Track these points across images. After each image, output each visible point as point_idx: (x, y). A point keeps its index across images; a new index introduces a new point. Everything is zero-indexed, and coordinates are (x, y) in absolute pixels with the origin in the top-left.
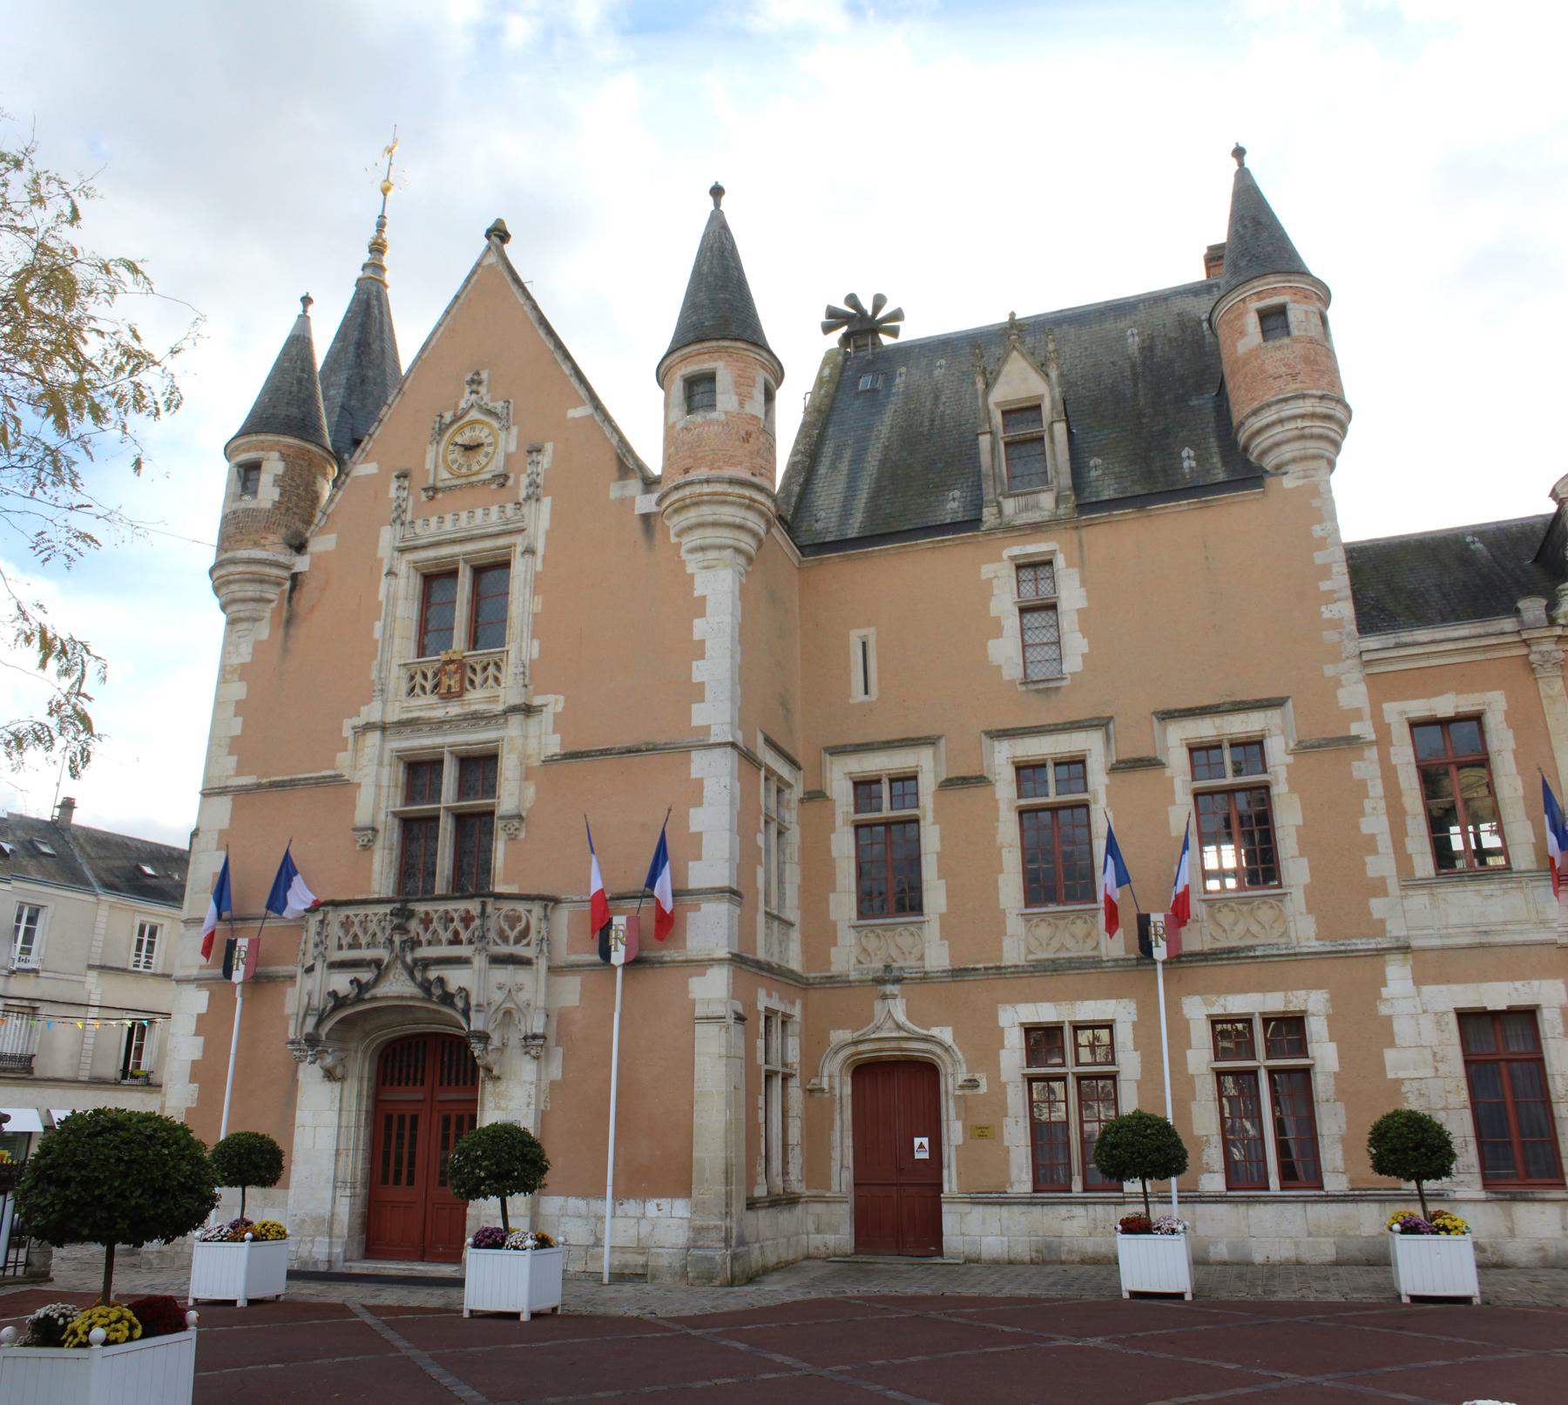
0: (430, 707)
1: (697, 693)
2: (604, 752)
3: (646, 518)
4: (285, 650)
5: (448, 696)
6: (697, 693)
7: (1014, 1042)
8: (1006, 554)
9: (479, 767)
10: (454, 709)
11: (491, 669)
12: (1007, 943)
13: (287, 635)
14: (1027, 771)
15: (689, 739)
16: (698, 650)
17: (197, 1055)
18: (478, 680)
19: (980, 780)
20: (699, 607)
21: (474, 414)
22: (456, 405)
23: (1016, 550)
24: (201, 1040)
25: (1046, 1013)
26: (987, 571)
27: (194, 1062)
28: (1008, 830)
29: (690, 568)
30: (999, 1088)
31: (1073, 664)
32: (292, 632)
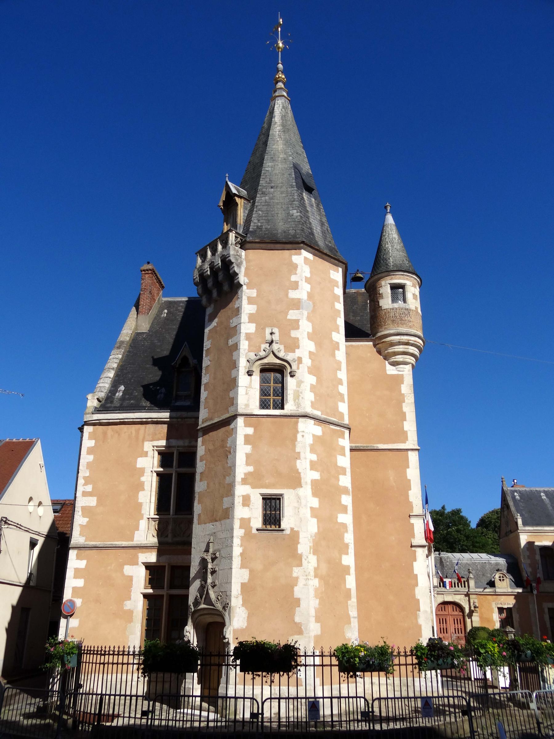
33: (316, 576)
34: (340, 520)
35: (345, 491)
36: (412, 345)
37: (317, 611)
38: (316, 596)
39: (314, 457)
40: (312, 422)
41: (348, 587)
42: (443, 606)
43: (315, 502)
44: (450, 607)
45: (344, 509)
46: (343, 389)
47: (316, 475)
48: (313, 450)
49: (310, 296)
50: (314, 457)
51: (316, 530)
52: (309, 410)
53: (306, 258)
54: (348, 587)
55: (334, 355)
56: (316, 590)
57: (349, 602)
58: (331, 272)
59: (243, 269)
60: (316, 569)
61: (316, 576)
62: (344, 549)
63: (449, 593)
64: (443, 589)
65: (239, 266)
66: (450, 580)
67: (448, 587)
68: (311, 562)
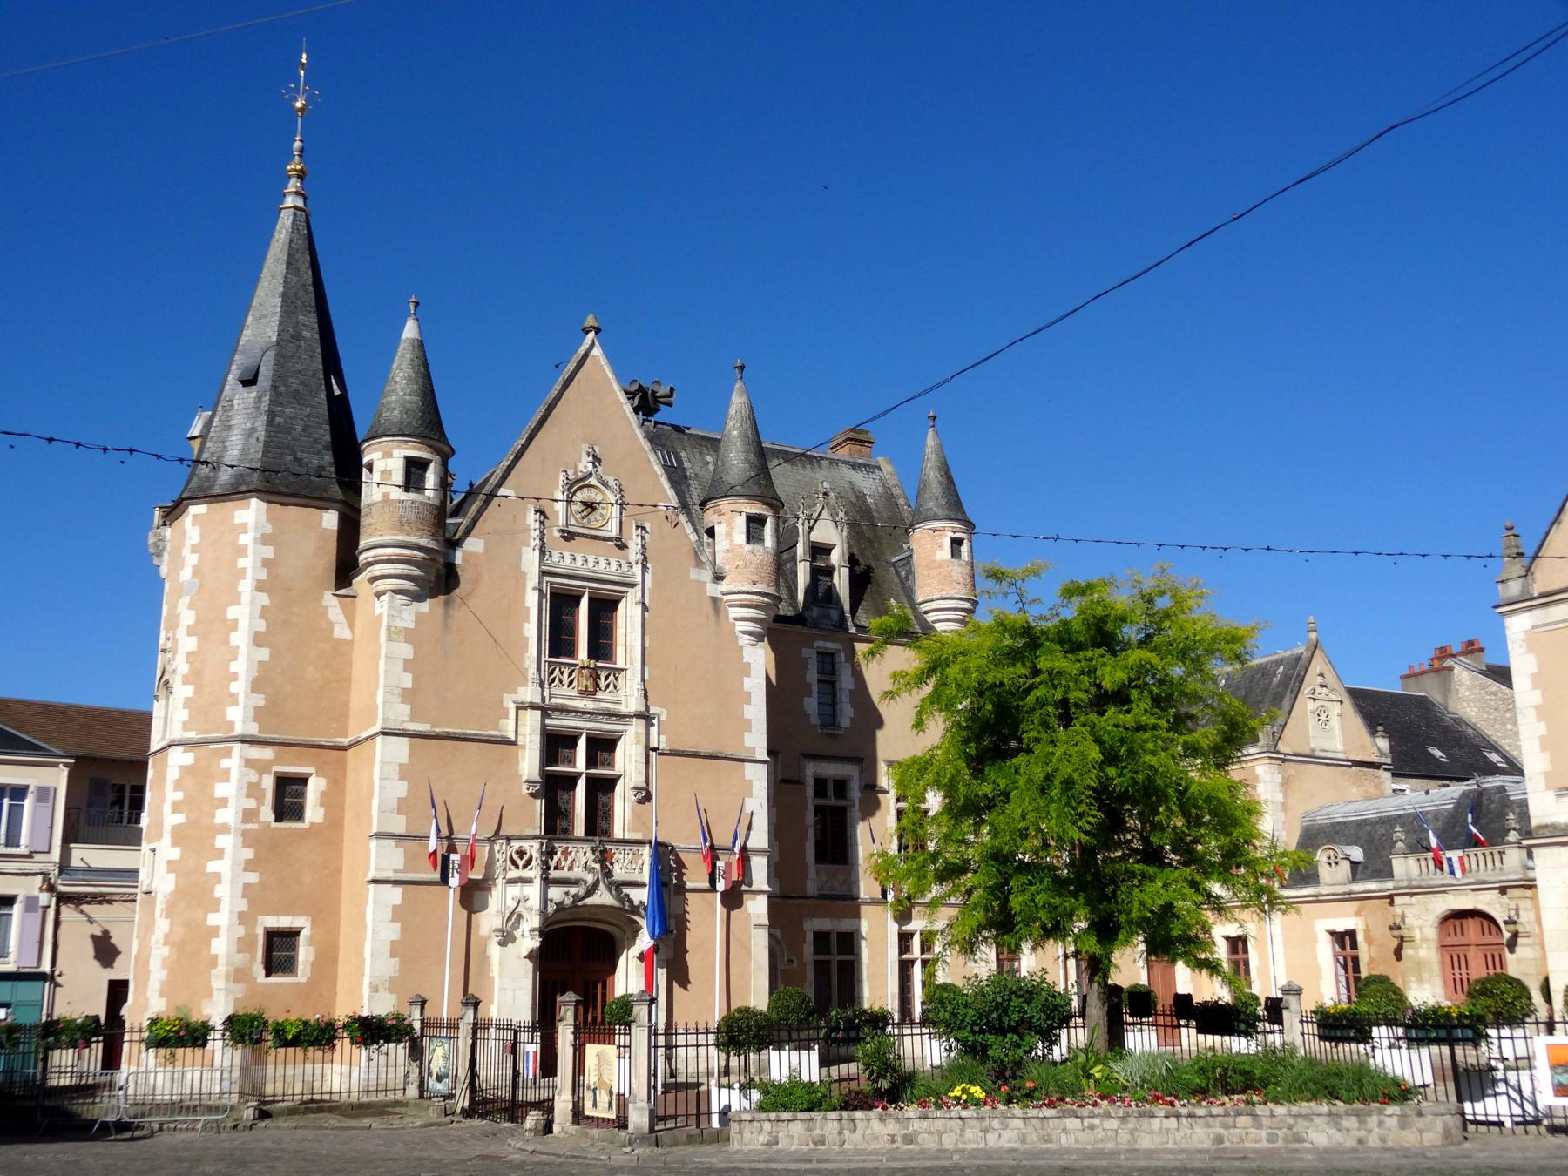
0: (570, 698)
1: (747, 725)
2: (696, 755)
3: (714, 600)
4: (446, 627)
5: (585, 693)
6: (747, 725)
7: (810, 938)
8: (816, 644)
9: (602, 747)
10: (590, 705)
11: (611, 678)
12: (809, 883)
13: (446, 614)
14: (820, 784)
15: (743, 755)
16: (747, 698)
17: (396, 936)
18: (602, 684)
19: (798, 782)
20: (746, 670)
21: (593, 481)
22: (576, 468)
23: (820, 644)
24: (398, 925)
25: (825, 924)
26: (806, 652)
27: (392, 942)
28: (810, 817)
29: (741, 643)
30: (803, 965)
31: (845, 722)
32: (451, 612)
33: (165, 944)
34: (209, 870)
35: (225, 829)
36: (377, 562)
37: (163, 984)
38: (163, 967)
39: (179, 796)
40: (181, 749)
41: (213, 951)
42: (1458, 923)
43: (175, 854)
44: (1472, 925)
45: (220, 854)
46: (239, 687)
47: (180, 818)
48: (178, 786)
49: (196, 571)
50: (179, 796)
51: (172, 887)
52: (177, 733)
53: (195, 516)
54: (213, 951)
55: (226, 641)
56: (164, 960)
57: (213, 971)
58: (237, 513)
59: (166, 556)
60: (166, 935)
61: (165, 944)
62: (215, 905)
63: (1459, 889)
64: (1449, 880)
65: (159, 555)
66: (1459, 853)
67: (1458, 873)
68: (162, 925)
